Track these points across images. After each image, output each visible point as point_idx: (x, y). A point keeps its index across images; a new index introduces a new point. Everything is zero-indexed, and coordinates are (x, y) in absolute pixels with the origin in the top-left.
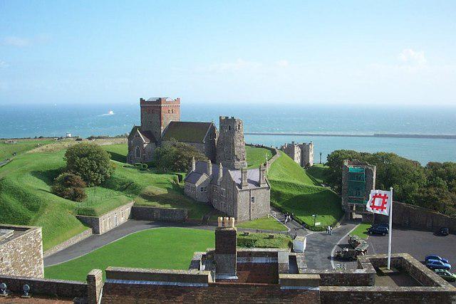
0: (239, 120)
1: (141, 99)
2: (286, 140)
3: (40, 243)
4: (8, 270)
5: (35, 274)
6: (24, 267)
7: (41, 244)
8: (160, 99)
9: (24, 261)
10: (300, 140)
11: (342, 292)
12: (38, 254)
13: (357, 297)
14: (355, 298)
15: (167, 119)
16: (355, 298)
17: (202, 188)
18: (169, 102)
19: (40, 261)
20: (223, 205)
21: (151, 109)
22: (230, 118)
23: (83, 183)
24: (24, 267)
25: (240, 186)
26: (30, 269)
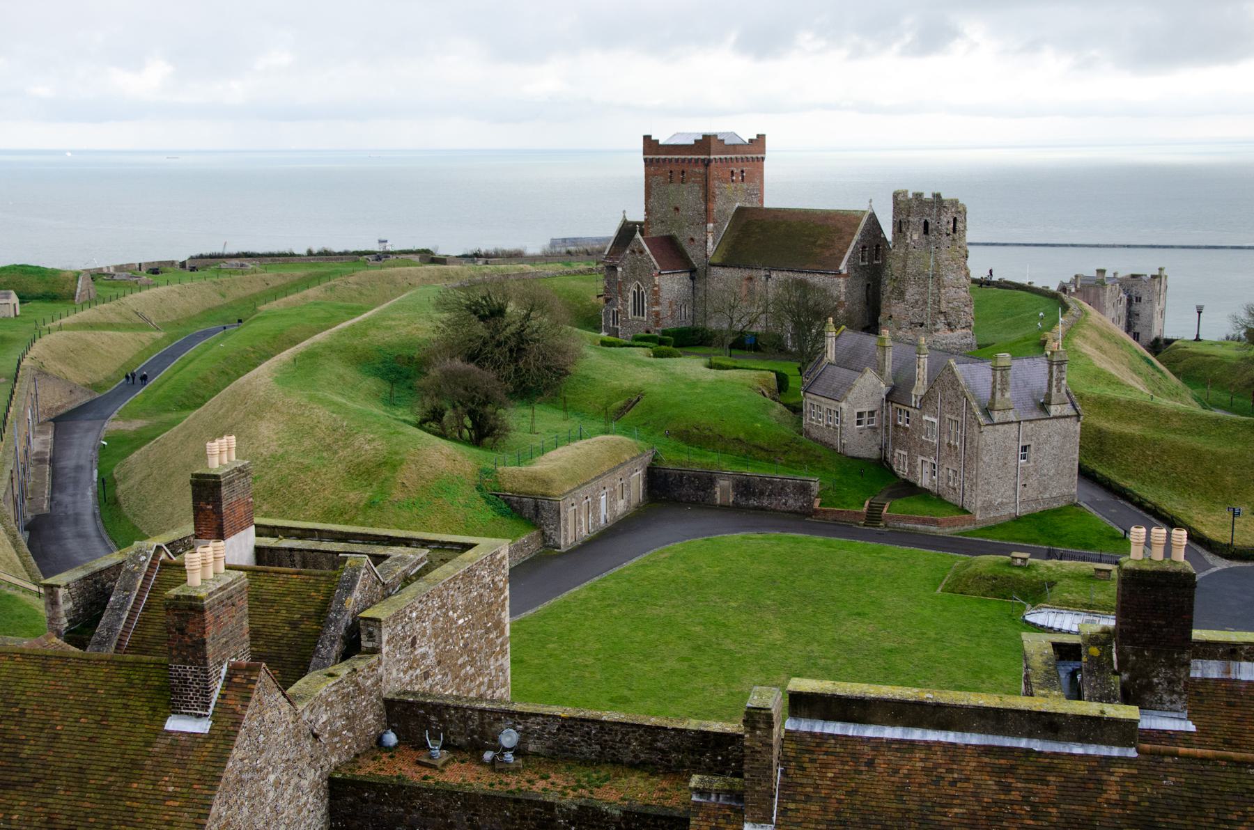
0: (954, 203)
1: (647, 139)
2: (1087, 266)
3: (502, 591)
4: (426, 675)
5: (490, 685)
6: (463, 666)
7: (507, 593)
9: (466, 645)
10: (1121, 265)
12: (498, 625)
15: (729, 199)
17: (860, 415)
18: (734, 148)
19: (502, 645)
20: (927, 468)
21: (683, 168)
22: (928, 195)
24: (463, 666)
25: (987, 411)
26: (479, 672)
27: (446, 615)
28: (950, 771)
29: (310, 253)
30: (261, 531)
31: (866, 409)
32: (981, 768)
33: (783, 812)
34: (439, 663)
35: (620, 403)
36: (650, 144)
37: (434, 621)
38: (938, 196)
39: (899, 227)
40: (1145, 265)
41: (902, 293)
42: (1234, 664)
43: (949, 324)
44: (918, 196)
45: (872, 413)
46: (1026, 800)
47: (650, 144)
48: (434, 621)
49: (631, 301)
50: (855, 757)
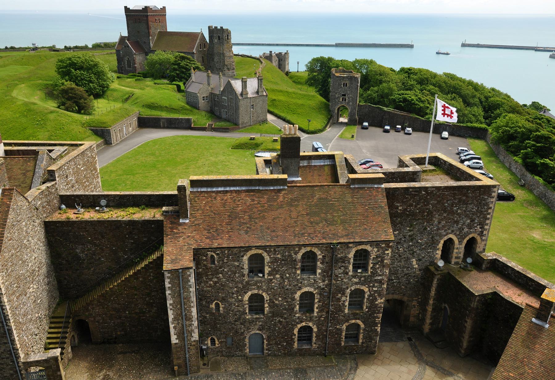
1: (126, 7)
2: (266, 50)
4: (73, 187)
8: (146, 7)
10: (276, 50)
11: (402, 188)
13: (415, 191)
14: (413, 193)
16: (413, 193)
17: (203, 97)
18: (156, 11)
19: (97, 175)
22: (219, 28)
23: (85, 95)
26: (91, 184)
27: (77, 167)
28: (237, 198)
29: (6, 48)
30: (5, 144)
31: (205, 95)
32: (246, 196)
33: (191, 214)
34: (77, 182)
35: (127, 96)
36: (127, 9)
37: (73, 169)
38: (222, 28)
39: (211, 37)
40: (283, 50)
41: (213, 59)
42: (310, 161)
43: (228, 69)
44: (216, 27)
45: (207, 97)
46: (259, 203)
47: (127, 9)
48: (73, 169)
49: (126, 63)
50: (211, 197)
